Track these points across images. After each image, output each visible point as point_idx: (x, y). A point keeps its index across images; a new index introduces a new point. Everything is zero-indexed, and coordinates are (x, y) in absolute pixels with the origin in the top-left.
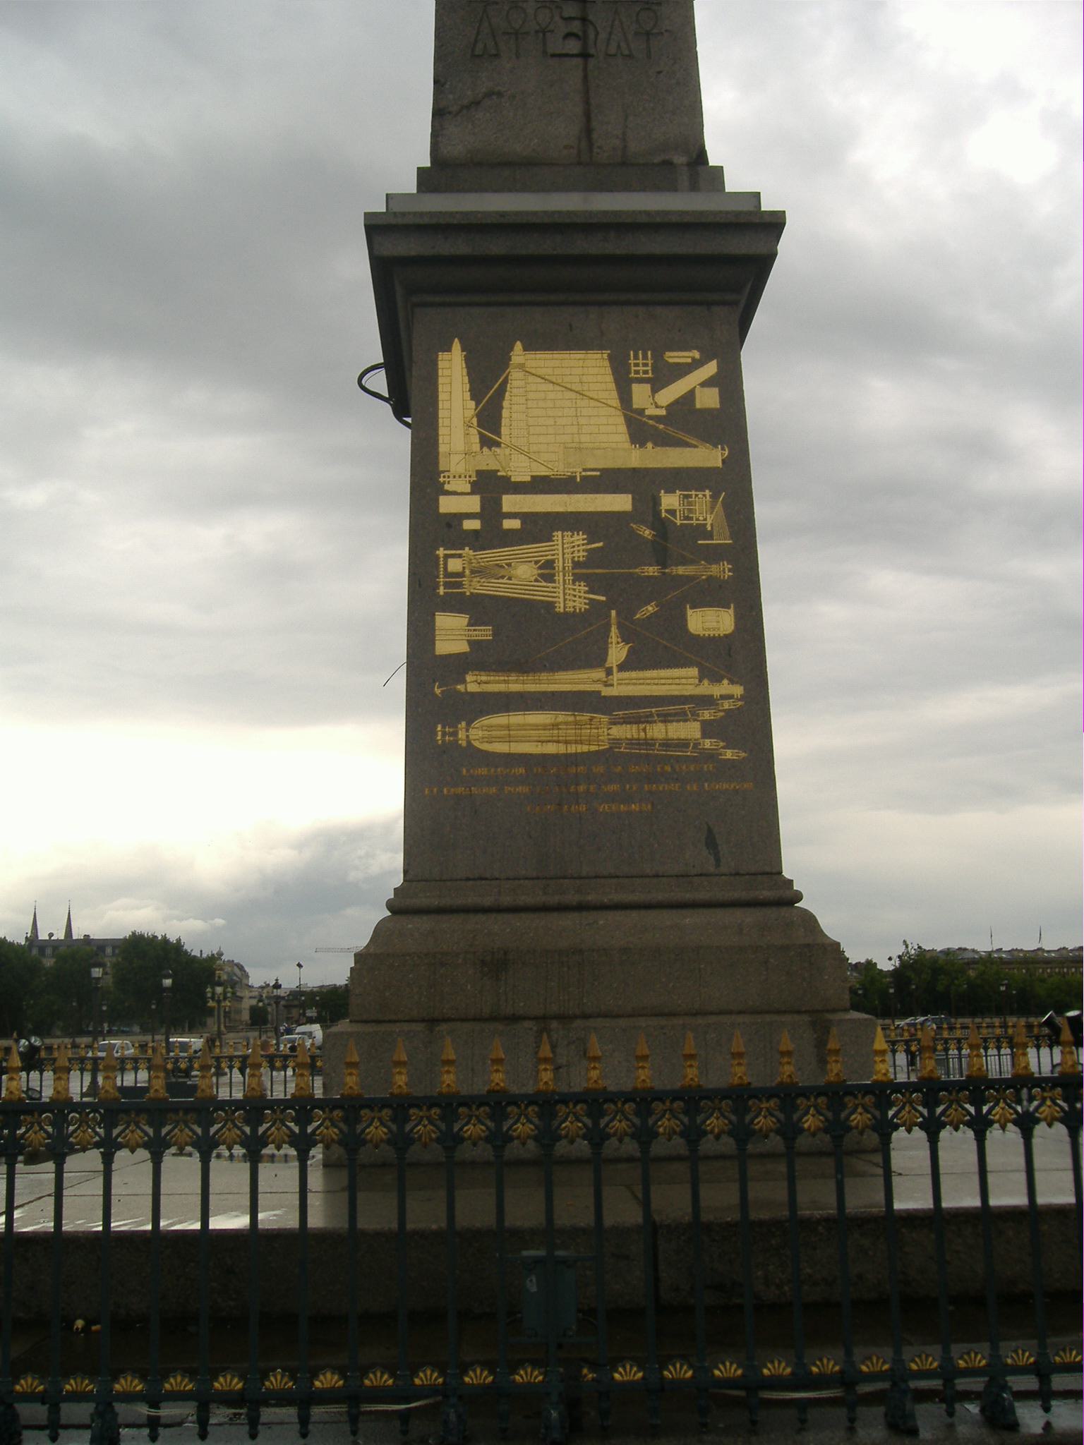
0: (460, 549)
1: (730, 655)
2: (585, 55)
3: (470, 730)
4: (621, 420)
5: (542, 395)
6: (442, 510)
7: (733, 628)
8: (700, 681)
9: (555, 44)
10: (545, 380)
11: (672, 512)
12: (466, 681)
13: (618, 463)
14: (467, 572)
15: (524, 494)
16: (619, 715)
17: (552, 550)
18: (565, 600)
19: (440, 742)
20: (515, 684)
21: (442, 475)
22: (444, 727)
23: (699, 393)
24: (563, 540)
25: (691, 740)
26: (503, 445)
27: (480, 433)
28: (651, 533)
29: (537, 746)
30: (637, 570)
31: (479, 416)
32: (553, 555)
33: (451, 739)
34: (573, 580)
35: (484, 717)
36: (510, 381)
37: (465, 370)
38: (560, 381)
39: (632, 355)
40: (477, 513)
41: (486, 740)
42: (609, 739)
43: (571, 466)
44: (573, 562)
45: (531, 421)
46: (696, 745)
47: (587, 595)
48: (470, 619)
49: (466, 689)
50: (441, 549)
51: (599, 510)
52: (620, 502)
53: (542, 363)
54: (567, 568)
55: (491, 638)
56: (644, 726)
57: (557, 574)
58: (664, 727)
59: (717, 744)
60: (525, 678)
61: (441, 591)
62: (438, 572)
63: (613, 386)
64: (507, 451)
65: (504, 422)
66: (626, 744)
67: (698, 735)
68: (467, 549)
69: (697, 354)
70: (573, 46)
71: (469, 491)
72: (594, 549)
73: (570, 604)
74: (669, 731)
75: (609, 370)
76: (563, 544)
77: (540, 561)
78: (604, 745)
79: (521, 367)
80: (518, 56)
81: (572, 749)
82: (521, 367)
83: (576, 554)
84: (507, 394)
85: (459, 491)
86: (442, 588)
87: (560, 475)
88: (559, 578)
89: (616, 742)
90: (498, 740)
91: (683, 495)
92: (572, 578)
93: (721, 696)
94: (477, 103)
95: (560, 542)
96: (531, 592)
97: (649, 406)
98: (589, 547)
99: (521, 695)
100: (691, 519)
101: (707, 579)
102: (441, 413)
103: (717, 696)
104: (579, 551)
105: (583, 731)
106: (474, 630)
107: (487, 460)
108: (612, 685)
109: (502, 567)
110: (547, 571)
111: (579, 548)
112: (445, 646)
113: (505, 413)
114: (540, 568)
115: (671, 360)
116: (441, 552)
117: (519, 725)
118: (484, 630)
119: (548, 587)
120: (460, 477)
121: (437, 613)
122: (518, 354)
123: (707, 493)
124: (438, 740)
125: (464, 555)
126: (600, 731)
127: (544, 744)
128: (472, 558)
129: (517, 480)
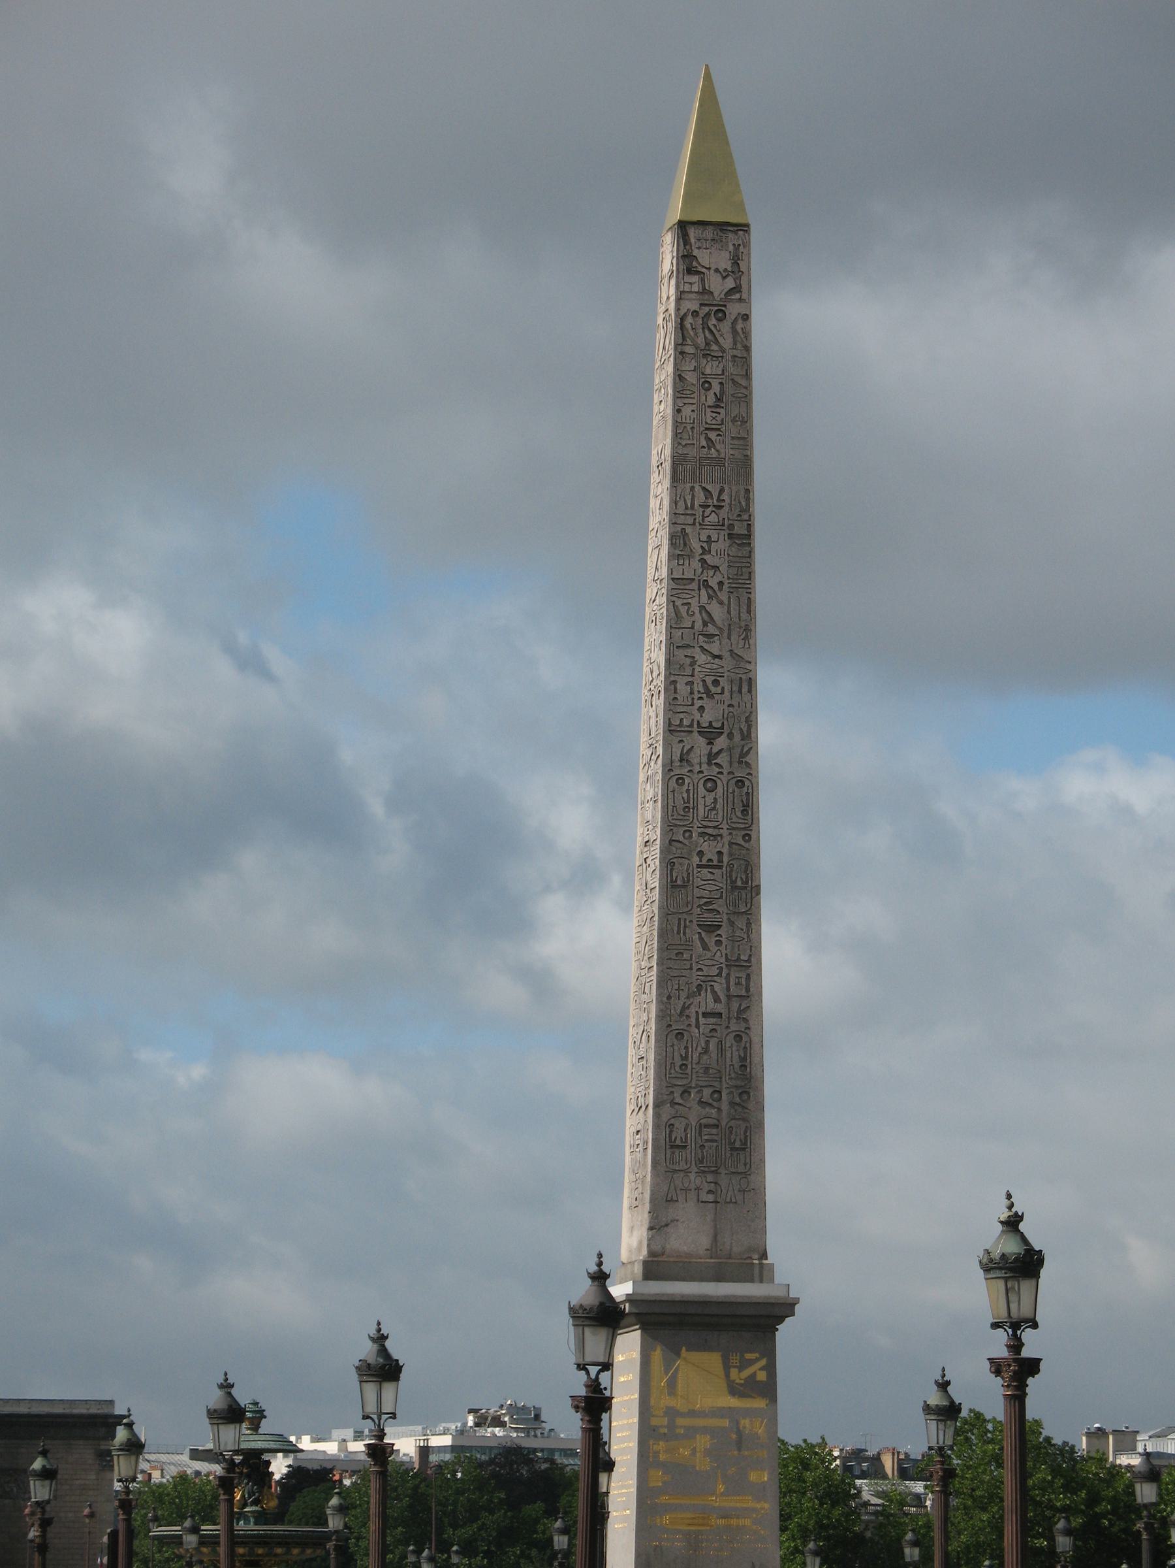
2: (716, 1202)
23: (758, 1372)
52: (726, 1423)
63: (722, 1369)
69: (757, 1355)
70: (711, 1198)
75: (721, 1361)
94: (667, 1225)
110: (694, 1451)
112: (652, 1484)
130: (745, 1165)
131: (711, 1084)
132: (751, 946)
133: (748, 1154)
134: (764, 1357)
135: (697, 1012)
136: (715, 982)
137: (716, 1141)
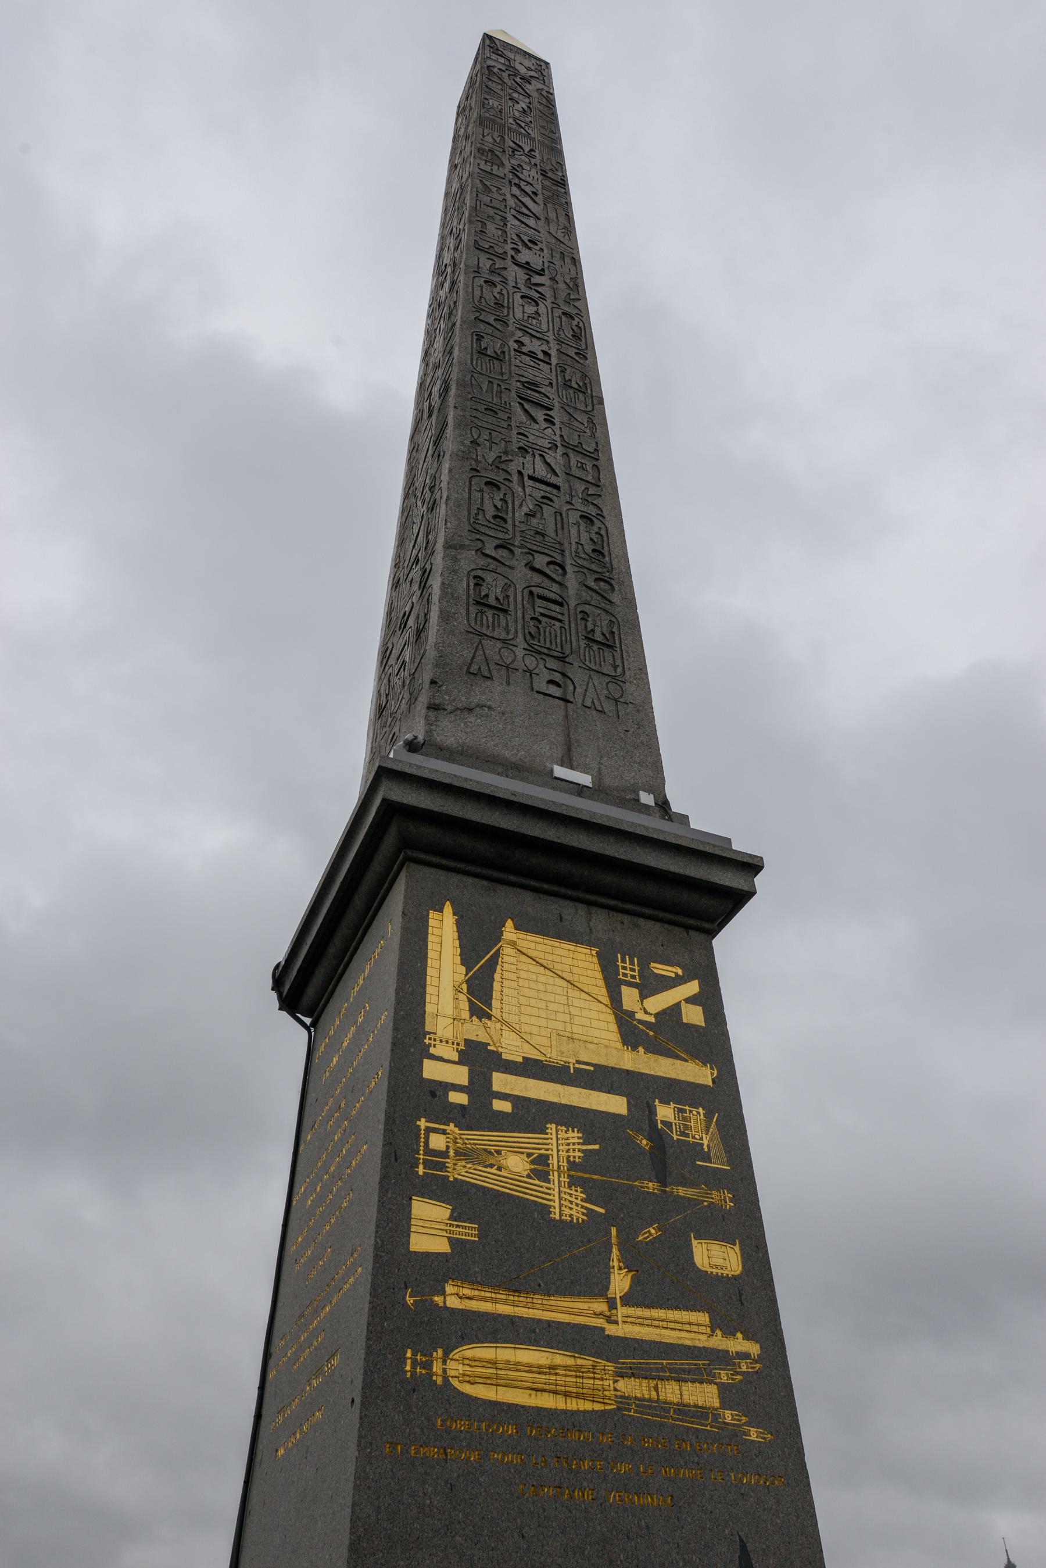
0: (444, 1124)
1: (742, 1304)
3: (449, 1361)
4: (612, 1018)
5: (534, 977)
6: (426, 1075)
7: (740, 1268)
8: (713, 1331)
9: (541, 684)
10: (537, 962)
11: (668, 1124)
12: (445, 1292)
13: (612, 1063)
14: (452, 1153)
15: (516, 1075)
16: (627, 1364)
17: (546, 1144)
18: (561, 1205)
19: (409, 1374)
20: (504, 1306)
21: (428, 1036)
22: (414, 1354)
24: (557, 1134)
25: (709, 1409)
26: (493, 1018)
27: (469, 1000)
28: (647, 1144)
29: (530, 1395)
30: (636, 1183)
31: (467, 982)
32: (547, 1150)
33: (423, 1372)
34: (569, 1183)
35: (466, 1345)
36: (501, 956)
37: (456, 934)
38: (550, 967)
39: (619, 958)
40: (465, 1086)
41: (467, 1379)
42: (616, 1396)
43: (564, 1055)
44: (568, 1161)
45: (523, 1000)
46: (716, 1417)
47: (585, 1204)
48: (453, 1211)
49: (445, 1303)
50: (423, 1120)
51: (594, 1108)
52: (616, 1104)
53: (532, 945)
54: (562, 1168)
55: (477, 1239)
56: (655, 1382)
57: (551, 1173)
58: (678, 1387)
59: (739, 1418)
60: (516, 1298)
61: (421, 1170)
62: (418, 1146)
64: (498, 1025)
65: (496, 995)
66: (637, 1406)
67: (716, 1403)
68: (452, 1125)
69: (680, 972)
71: (456, 1059)
72: (590, 1151)
73: (567, 1211)
74: (684, 1393)
75: (598, 967)
76: (557, 1139)
77: (533, 1154)
78: (610, 1404)
79: (513, 944)
80: (508, 684)
81: (573, 1405)
82: (513, 944)
83: (571, 1154)
84: (499, 967)
85: (446, 1057)
86: (421, 1167)
87: (553, 1062)
88: (554, 1177)
89: (624, 1401)
90: (481, 1380)
91: (678, 1108)
92: (568, 1180)
93: (737, 1353)
94: (470, 710)
95: (554, 1136)
96: (523, 1190)
97: (638, 1010)
98: (585, 1147)
99: (512, 1321)
100: (687, 1136)
101: (709, 1206)
102: (429, 971)
103: (732, 1352)
104: (574, 1150)
105: (585, 1381)
106: (458, 1226)
107: (476, 1031)
108: (616, 1323)
109: (493, 1154)
110: (540, 1167)
111: (574, 1147)
113: (496, 986)
114: (532, 1162)
115: (656, 971)
116: (423, 1123)
117: (508, 1362)
118: (469, 1227)
119: (542, 1187)
120: (447, 1042)
121: (414, 1198)
122: (509, 932)
123: (701, 1110)
124: (407, 1371)
125: (448, 1131)
126: (606, 1383)
127: (539, 1393)
128: (458, 1137)
129: (508, 1058)
130: (615, 667)
131: (546, 551)
132: (597, 443)
133: (618, 655)
134: (693, 979)
135: (520, 473)
136: (545, 452)
137: (560, 621)
